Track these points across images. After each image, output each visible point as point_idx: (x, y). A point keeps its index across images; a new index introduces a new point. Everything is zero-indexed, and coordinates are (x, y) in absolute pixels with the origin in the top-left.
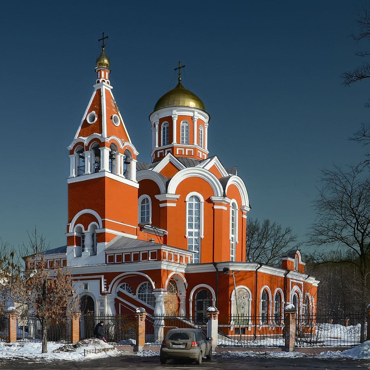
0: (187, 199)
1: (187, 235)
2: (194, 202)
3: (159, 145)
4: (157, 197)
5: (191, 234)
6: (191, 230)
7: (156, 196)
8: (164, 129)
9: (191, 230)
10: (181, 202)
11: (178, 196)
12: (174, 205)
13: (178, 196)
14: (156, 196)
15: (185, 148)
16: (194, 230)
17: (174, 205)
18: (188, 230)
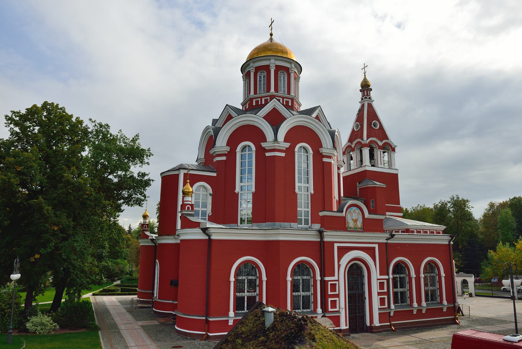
0: (296, 149)
1: (297, 190)
2: (303, 153)
3: (255, 93)
4: (264, 145)
5: (300, 188)
6: (300, 185)
7: (262, 144)
8: (260, 77)
9: (300, 185)
10: (290, 152)
11: (287, 145)
12: (283, 155)
13: (287, 145)
14: (262, 144)
15: (283, 98)
16: (303, 185)
17: (283, 155)
18: (297, 184)
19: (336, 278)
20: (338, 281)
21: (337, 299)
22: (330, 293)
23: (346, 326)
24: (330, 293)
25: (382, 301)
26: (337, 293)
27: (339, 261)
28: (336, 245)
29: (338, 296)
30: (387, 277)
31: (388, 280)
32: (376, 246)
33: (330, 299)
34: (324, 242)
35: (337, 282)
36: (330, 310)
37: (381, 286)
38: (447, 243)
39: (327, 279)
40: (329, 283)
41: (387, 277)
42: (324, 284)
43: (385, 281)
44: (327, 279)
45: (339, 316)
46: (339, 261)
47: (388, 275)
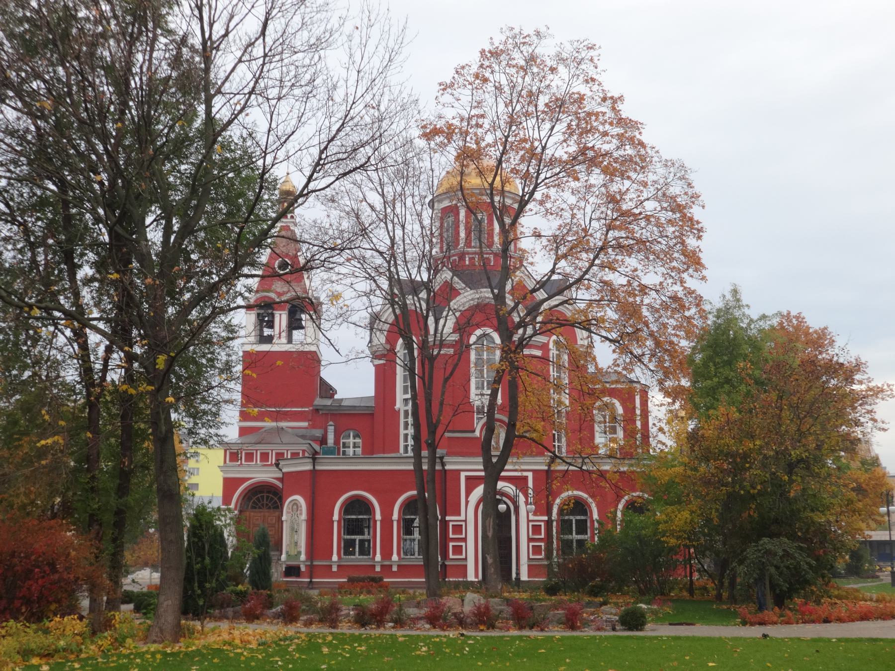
19: (463, 517)
20: (465, 521)
21: (463, 544)
22: (451, 536)
23: (476, 576)
24: (451, 536)
25: (537, 550)
26: (463, 536)
27: (467, 496)
28: (463, 475)
29: (465, 540)
30: (546, 518)
31: (549, 523)
32: (530, 475)
33: (451, 544)
34: (446, 471)
35: (463, 524)
36: (451, 556)
37: (536, 529)
38: (546, 468)
39: (448, 518)
40: (451, 524)
41: (546, 518)
42: (445, 524)
43: (542, 524)
44: (448, 518)
45: (466, 566)
46: (467, 496)
47: (549, 513)
